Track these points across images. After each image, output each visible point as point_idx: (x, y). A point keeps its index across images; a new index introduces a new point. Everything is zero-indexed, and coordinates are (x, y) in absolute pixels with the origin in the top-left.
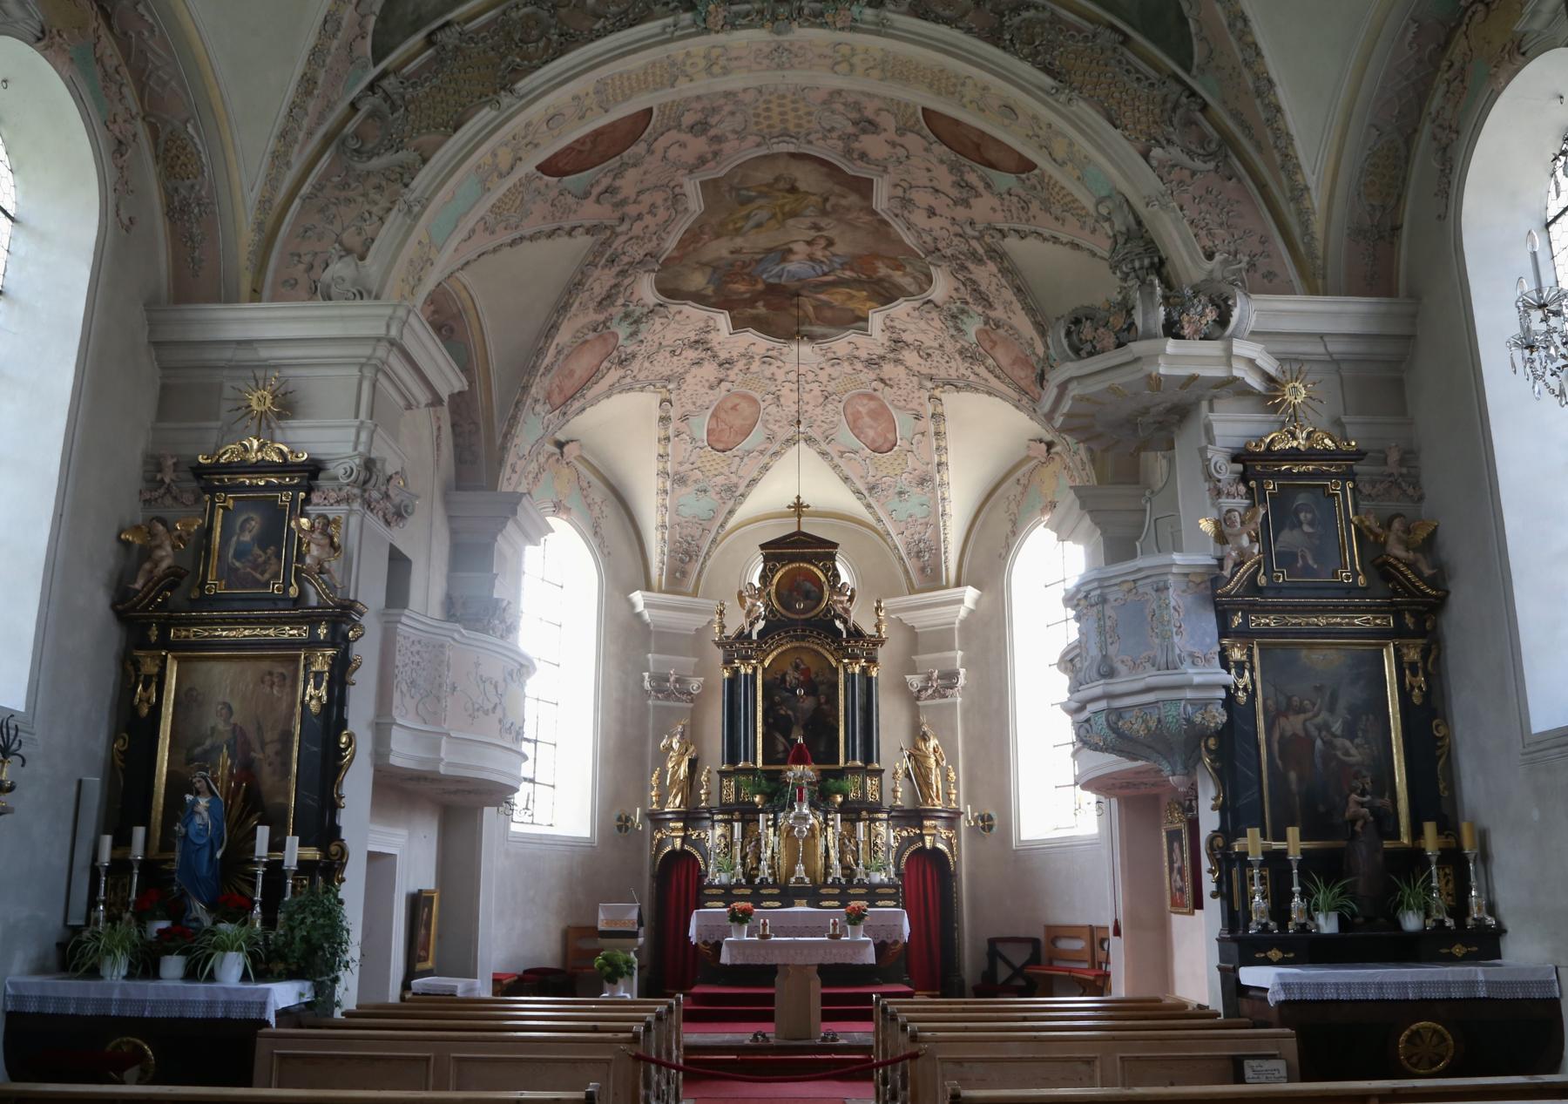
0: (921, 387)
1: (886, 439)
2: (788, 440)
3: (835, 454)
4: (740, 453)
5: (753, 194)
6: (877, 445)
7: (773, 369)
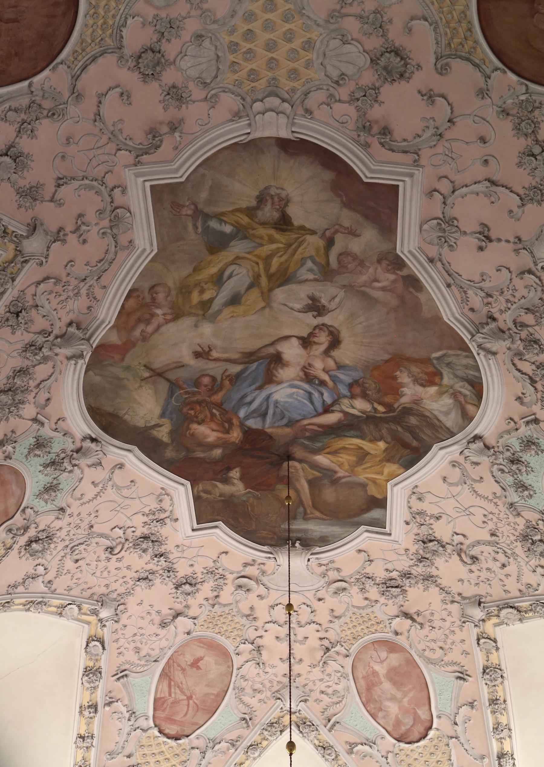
0: (465, 619)
1: (416, 718)
2: (271, 724)
3: (341, 749)
4: (201, 743)
5: (228, 229)
6: (403, 729)
7: (252, 597)
